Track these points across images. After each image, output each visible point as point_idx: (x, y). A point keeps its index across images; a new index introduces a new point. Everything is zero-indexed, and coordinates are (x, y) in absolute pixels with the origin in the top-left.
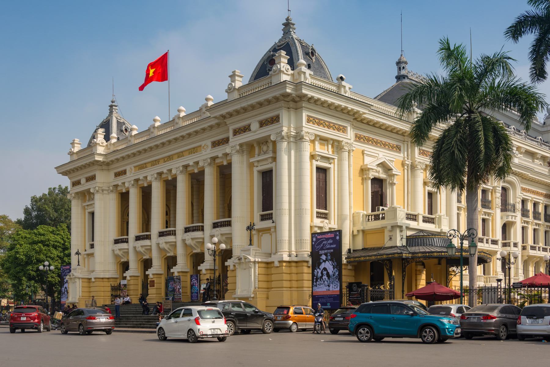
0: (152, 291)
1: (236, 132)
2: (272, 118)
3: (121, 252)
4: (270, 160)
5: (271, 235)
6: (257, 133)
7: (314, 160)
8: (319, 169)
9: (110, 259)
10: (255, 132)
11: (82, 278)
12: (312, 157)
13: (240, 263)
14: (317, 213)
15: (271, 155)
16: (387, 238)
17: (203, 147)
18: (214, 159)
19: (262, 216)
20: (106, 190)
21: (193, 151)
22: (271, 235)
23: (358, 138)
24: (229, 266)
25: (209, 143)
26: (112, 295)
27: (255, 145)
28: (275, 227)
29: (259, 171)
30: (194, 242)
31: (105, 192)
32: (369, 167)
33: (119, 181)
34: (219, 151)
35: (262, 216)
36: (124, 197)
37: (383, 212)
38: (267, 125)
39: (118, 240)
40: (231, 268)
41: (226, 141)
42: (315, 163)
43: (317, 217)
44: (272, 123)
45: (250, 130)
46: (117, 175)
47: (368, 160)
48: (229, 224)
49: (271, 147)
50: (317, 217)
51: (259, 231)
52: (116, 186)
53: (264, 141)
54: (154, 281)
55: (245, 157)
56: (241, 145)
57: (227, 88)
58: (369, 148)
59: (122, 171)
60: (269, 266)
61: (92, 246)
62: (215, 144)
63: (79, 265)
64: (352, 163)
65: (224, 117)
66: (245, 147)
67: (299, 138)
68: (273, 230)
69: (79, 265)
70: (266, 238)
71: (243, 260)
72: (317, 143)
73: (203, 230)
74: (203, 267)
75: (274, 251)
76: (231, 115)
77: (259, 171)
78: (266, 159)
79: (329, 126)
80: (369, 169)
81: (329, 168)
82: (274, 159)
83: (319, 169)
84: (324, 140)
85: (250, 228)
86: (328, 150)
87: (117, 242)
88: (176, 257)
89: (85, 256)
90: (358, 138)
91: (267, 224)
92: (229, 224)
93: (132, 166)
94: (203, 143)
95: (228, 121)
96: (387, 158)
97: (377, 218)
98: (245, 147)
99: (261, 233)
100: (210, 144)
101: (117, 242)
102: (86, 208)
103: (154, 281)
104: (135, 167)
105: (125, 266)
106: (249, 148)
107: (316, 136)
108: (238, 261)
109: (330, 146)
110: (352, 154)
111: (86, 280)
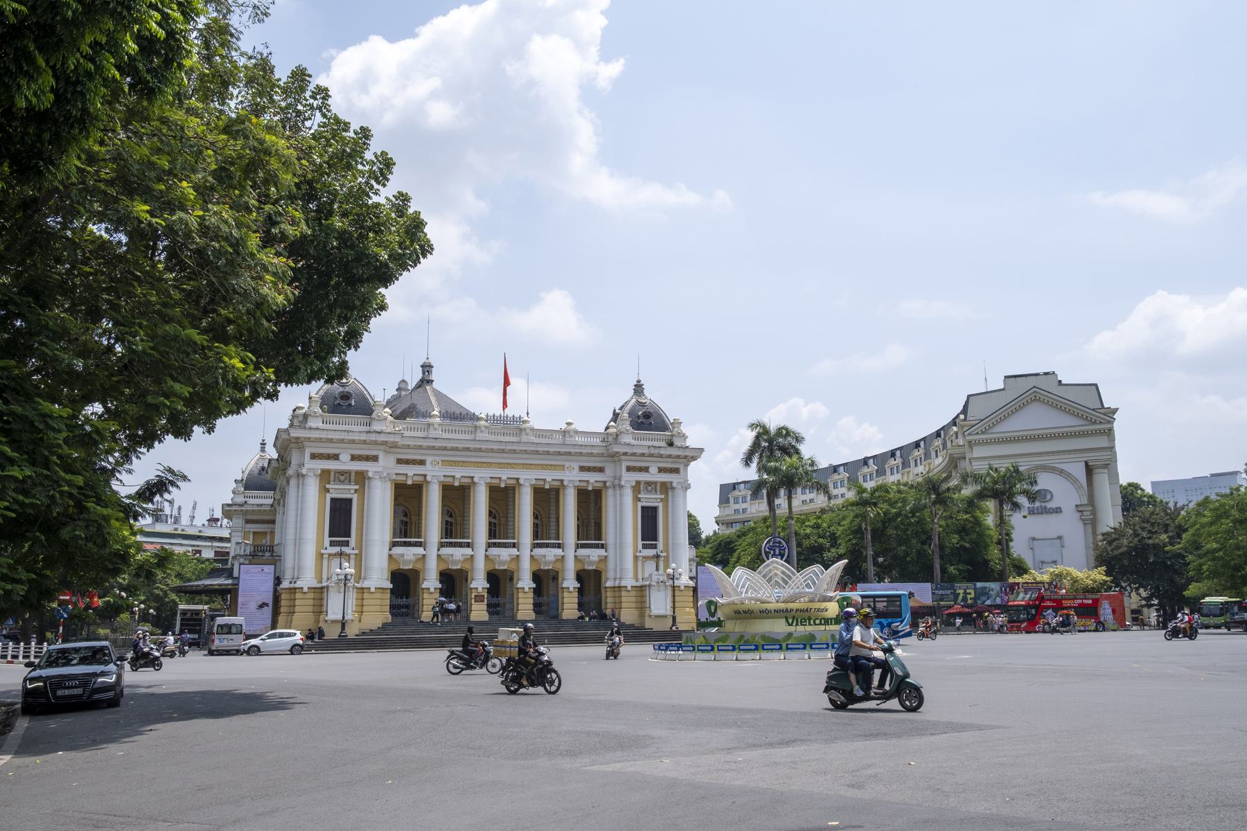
1: (629, 469)
25: (576, 466)
62: (582, 469)
65: (625, 454)
93: (438, 459)
94: (567, 464)
100: (577, 469)
101: (394, 544)
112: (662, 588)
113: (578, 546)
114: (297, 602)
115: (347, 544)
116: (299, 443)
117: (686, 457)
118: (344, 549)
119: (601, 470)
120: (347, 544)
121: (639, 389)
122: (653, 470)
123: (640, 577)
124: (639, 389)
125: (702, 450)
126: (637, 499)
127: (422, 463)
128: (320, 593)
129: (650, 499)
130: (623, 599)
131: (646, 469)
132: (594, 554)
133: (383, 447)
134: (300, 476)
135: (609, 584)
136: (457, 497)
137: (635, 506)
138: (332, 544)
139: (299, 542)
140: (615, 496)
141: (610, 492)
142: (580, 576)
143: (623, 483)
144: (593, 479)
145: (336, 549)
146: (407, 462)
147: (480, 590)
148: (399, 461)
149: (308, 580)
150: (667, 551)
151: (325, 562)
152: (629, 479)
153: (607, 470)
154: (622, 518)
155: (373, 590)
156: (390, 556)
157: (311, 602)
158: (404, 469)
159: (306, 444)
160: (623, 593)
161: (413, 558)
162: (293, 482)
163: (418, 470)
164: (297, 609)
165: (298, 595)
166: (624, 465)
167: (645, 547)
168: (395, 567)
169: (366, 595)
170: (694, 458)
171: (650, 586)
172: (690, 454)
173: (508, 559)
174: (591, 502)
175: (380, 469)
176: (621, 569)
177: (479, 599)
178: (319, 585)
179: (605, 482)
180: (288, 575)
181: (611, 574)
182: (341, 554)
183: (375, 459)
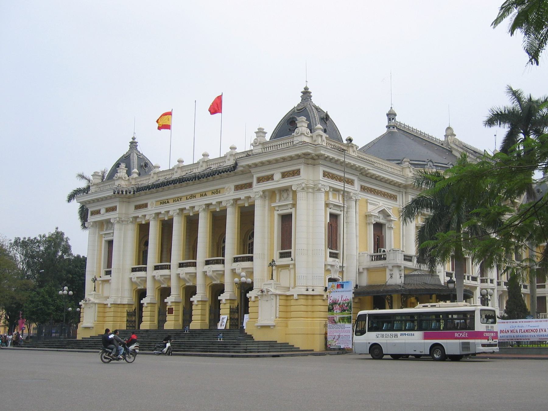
0: (169, 317)
1: (259, 180)
2: (293, 171)
3: (139, 280)
4: (290, 206)
5: (290, 270)
6: (278, 182)
7: (328, 208)
8: (332, 215)
9: (127, 286)
10: (278, 181)
11: (98, 304)
12: (327, 205)
13: (262, 296)
14: (330, 253)
15: (291, 202)
16: (388, 276)
18: (236, 200)
19: (281, 254)
20: (125, 221)
21: (217, 192)
22: (290, 270)
23: (363, 189)
24: (251, 297)
26: (127, 320)
27: (276, 192)
28: (294, 265)
29: (279, 215)
30: (215, 274)
31: (124, 222)
32: (372, 214)
33: (140, 213)
34: (242, 194)
35: (281, 254)
36: (143, 230)
37: (384, 253)
38: (288, 177)
39: (135, 268)
40: (253, 299)
41: (250, 185)
42: (329, 211)
43: (330, 256)
44: (293, 176)
45: (273, 179)
46: (138, 207)
47: (370, 208)
48: (251, 259)
49: (291, 196)
50: (330, 256)
51: (279, 267)
52: (136, 218)
53: (286, 190)
55: (267, 202)
56: (264, 192)
57: (252, 142)
58: (371, 198)
59: (143, 205)
60: (289, 298)
61: (108, 273)
62: (238, 188)
63: (95, 290)
64: (358, 211)
65: (249, 166)
66: (267, 193)
67: (316, 189)
68: (291, 266)
69: (95, 290)
70: (284, 274)
71: (265, 293)
72: (330, 193)
73: (223, 263)
74: (223, 297)
75: (292, 285)
76: (256, 165)
77: (279, 215)
78: (286, 205)
79: (340, 179)
80: (371, 215)
81: (340, 215)
82: (294, 205)
83: (332, 215)
84: (335, 190)
85: (272, 264)
86: (339, 200)
87: (134, 270)
88: (196, 287)
89: (100, 282)
90: (363, 189)
91: (286, 261)
92: (251, 259)
93: (154, 201)
94: (226, 186)
95: (253, 170)
96: (386, 206)
97: (379, 258)
98: (267, 193)
99: (280, 269)
100: (233, 188)
101: (134, 270)
102: (103, 236)
104: (157, 202)
105: (142, 294)
106: (271, 195)
107: (330, 187)
108: (260, 293)
109: (341, 196)
110: (358, 203)
111: (102, 306)
117: (299, 157)
121: (306, 94)
126: (272, 210)
127: (146, 206)
137: (271, 216)
174: (247, 216)
177: (171, 311)
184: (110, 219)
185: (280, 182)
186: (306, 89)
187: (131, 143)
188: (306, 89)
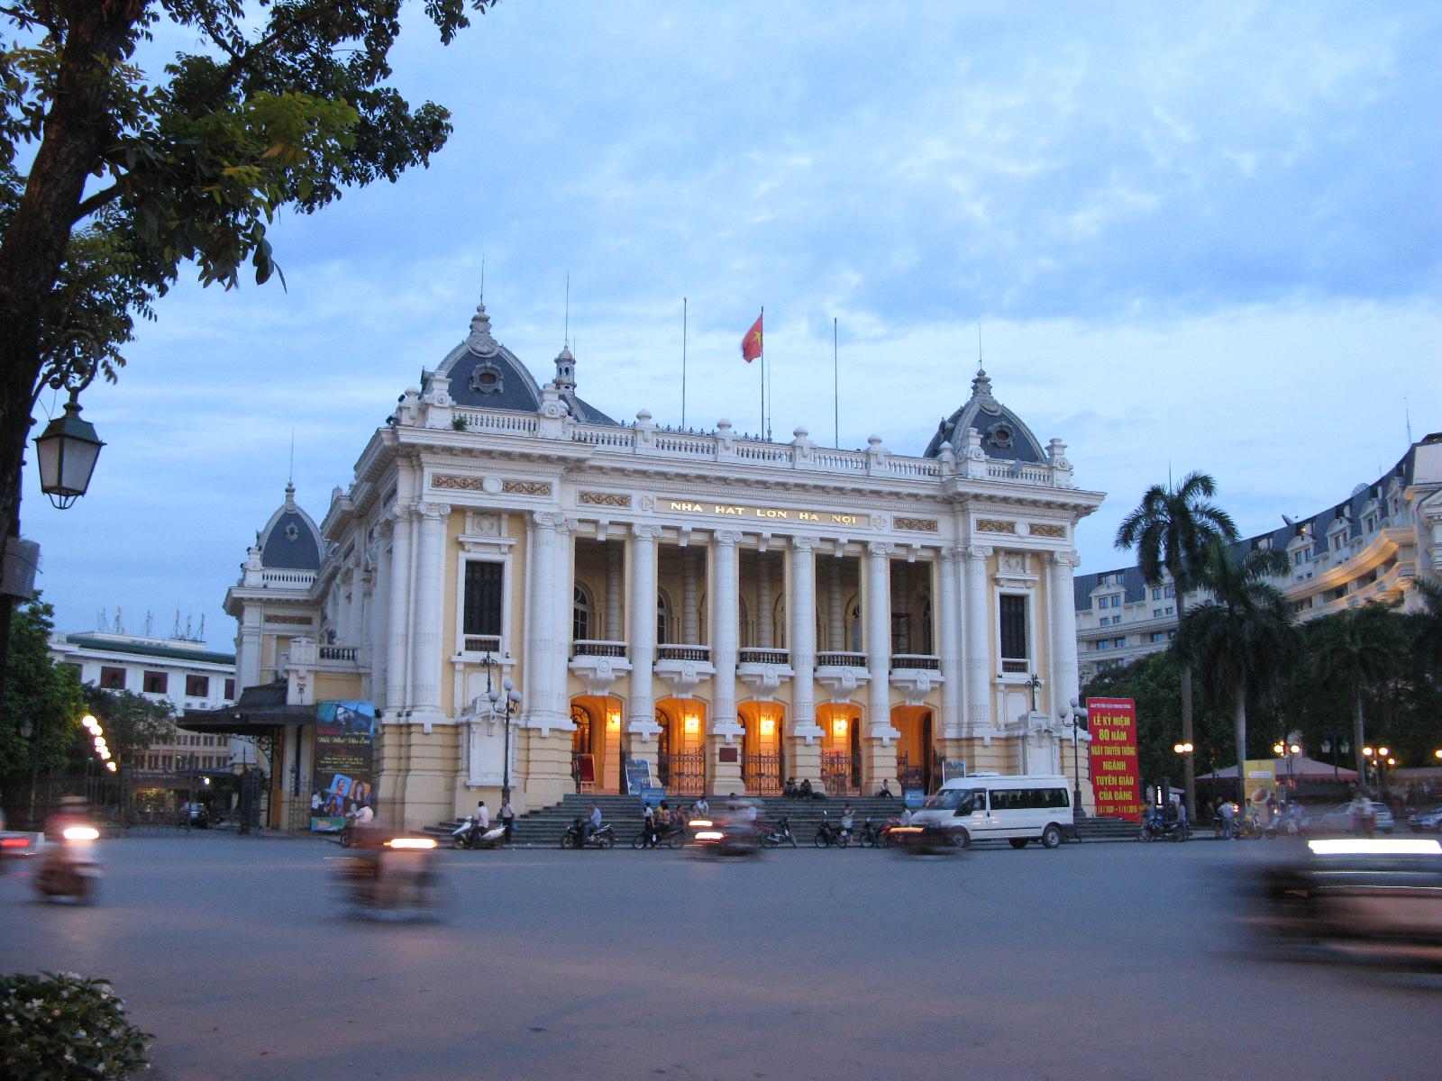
6: (1022, 538)
17: (875, 520)
25: (888, 517)
34: (917, 539)
35: (1004, 663)
38: (1041, 534)
54: (735, 750)
62: (900, 523)
65: (977, 497)
93: (651, 495)
95: (971, 505)
100: (890, 524)
101: (579, 650)
103: (735, 750)
112: (1046, 742)
113: (896, 664)
114: (414, 751)
115: (494, 646)
116: (412, 455)
117: (1076, 507)
118: (493, 655)
119: (931, 526)
120: (494, 646)
121: (981, 382)
122: (1022, 528)
123: (1001, 721)
124: (981, 382)
125: (1101, 496)
126: (995, 581)
127: (624, 501)
128: (457, 732)
129: (1017, 579)
130: (978, 762)
131: (1010, 528)
132: (925, 677)
133: (560, 469)
134: (415, 516)
135: (951, 733)
136: (683, 565)
138: (470, 645)
139: (414, 639)
140: (956, 573)
141: (948, 567)
142: (899, 716)
143: (971, 549)
144: (917, 539)
145: (478, 656)
146: (598, 499)
147: (730, 738)
148: (585, 497)
149: (431, 713)
150: (1046, 677)
151: (459, 678)
152: (983, 542)
153: (941, 526)
154: (966, 612)
155: (545, 732)
156: (570, 671)
157: (438, 752)
158: (592, 512)
159: (425, 457)
160: (978, 750)
161: (612, 676)
162: (401, 530)
163: (618, 514)
164: (414, 764)
165: (415, 738)
166: (974, 518)
167: (1008, 667)
168: (577, 690)
169: (534, 743)
170: (1088, 510)
171: (1024, 738)
172: (1083, 502)
173: (778, 683)
174: (912, 580)
175: (555, 510)
176: (971, 708)
178: (451, 721)
179: (937, 549)
180: (395, 699)
181: (952, 717)
182: (486, 664)
183: (544, 489)
184: (531, 513)
185: (1026, 540)
186: (981, 373)
187: (475, 319)
188: (981, 373)
